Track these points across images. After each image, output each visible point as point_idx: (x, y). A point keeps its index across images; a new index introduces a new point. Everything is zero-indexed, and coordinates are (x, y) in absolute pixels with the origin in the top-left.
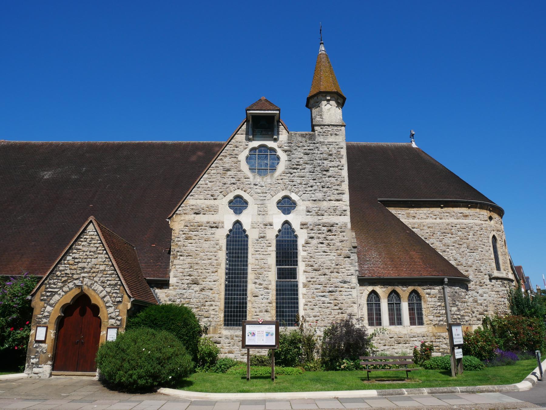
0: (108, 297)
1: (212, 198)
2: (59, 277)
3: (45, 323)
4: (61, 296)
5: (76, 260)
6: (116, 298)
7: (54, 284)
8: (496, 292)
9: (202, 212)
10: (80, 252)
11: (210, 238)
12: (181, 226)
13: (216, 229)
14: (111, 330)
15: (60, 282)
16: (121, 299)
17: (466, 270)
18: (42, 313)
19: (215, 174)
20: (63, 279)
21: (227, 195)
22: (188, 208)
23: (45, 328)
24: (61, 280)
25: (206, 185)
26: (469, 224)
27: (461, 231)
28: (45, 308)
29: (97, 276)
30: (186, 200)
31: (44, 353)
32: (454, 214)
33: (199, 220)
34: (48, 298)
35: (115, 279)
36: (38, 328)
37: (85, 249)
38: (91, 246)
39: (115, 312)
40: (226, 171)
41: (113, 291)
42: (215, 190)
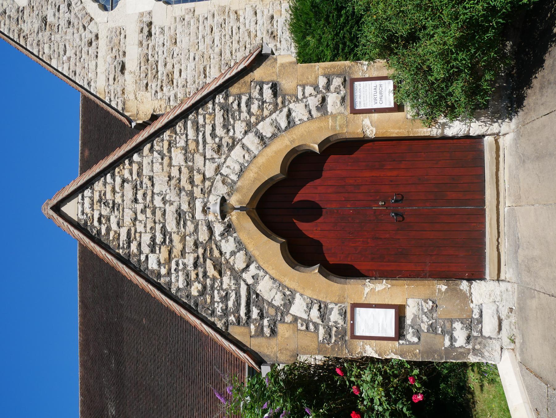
0: (260, 127)
1: (94, 44)
2: (204, 287)
3: (343, 314)
4: (261, 273)
5: (159, 238)
6: (263, 102)
7: (226, 298)
9: (122, 59)
10: (136, 231)
11: (170, 35)
12: (147, 98)
13: (153, 26)
14: (357, 100)
15: (222, 283)
16: (268, 84)
18: (311, 327)
19: (52, 44)
20: (211, 272)
21: (89, 15)
22: (112, 88)
23: (358, 310)
24: (214, 279)
25: (71, 59)
28: (296, 319)
29: (202, 168)
30: (98, 95)
31: (435, 306)
33: (136, 63)
34: (267, 313)
35: (210, 114)
36: (358, 333)
37: (128, 215)
38: (120, 202)
39: (304, 97)
40: (46, 25)
41: (244, 115)
42: (81, 40)
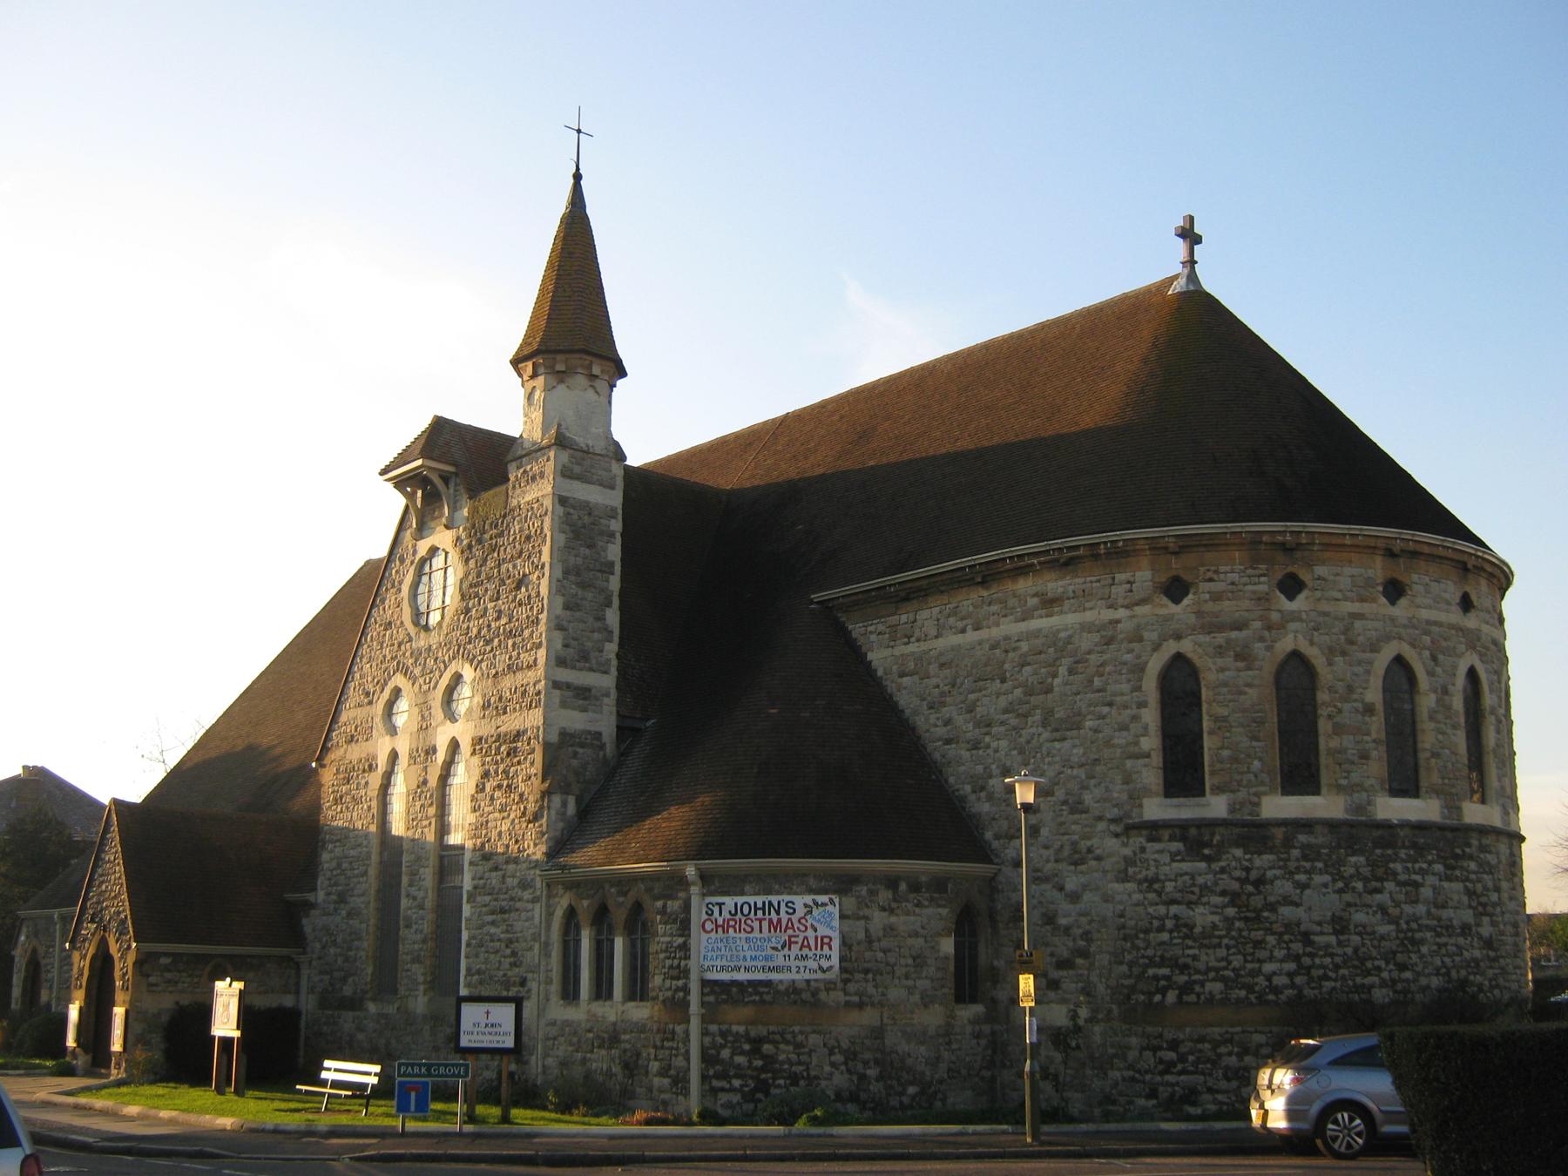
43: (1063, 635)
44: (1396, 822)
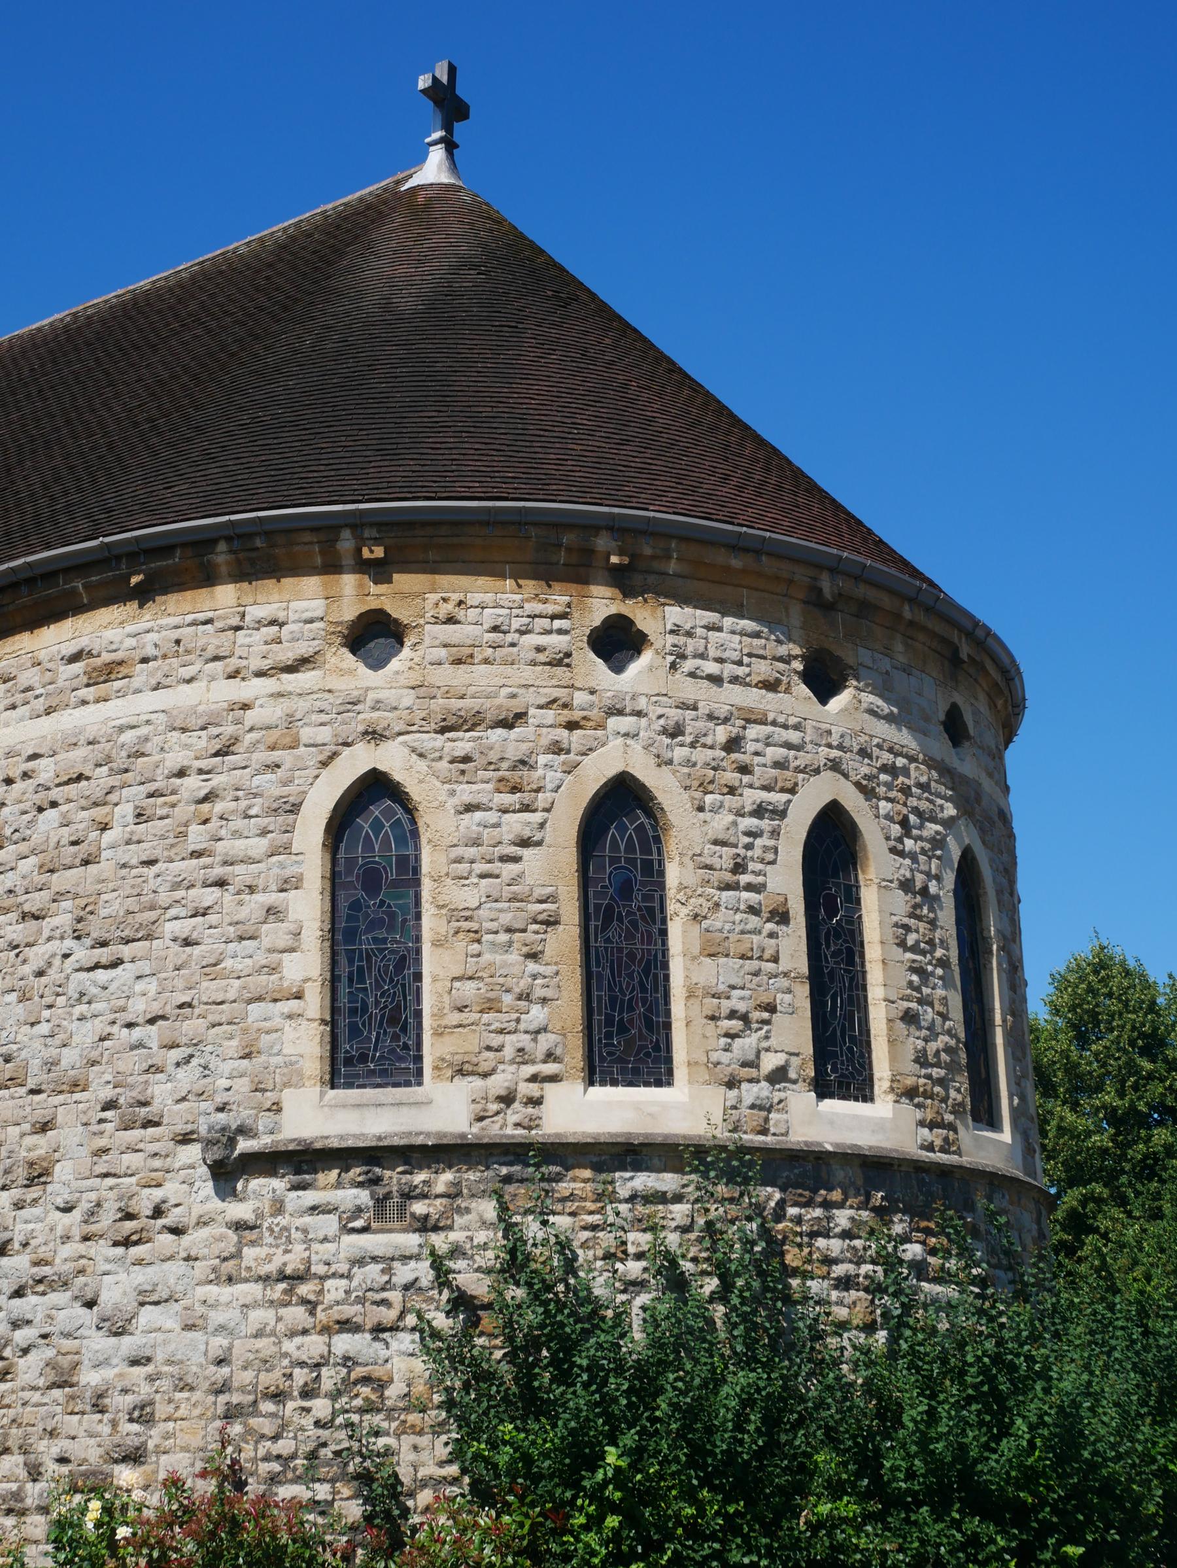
8: (265, 1279)
17: (41, 1115)
26: (121, 729)
27: (54, 804)
32: (29, 677)
43: (128, 737)
44: (830, 1148)
